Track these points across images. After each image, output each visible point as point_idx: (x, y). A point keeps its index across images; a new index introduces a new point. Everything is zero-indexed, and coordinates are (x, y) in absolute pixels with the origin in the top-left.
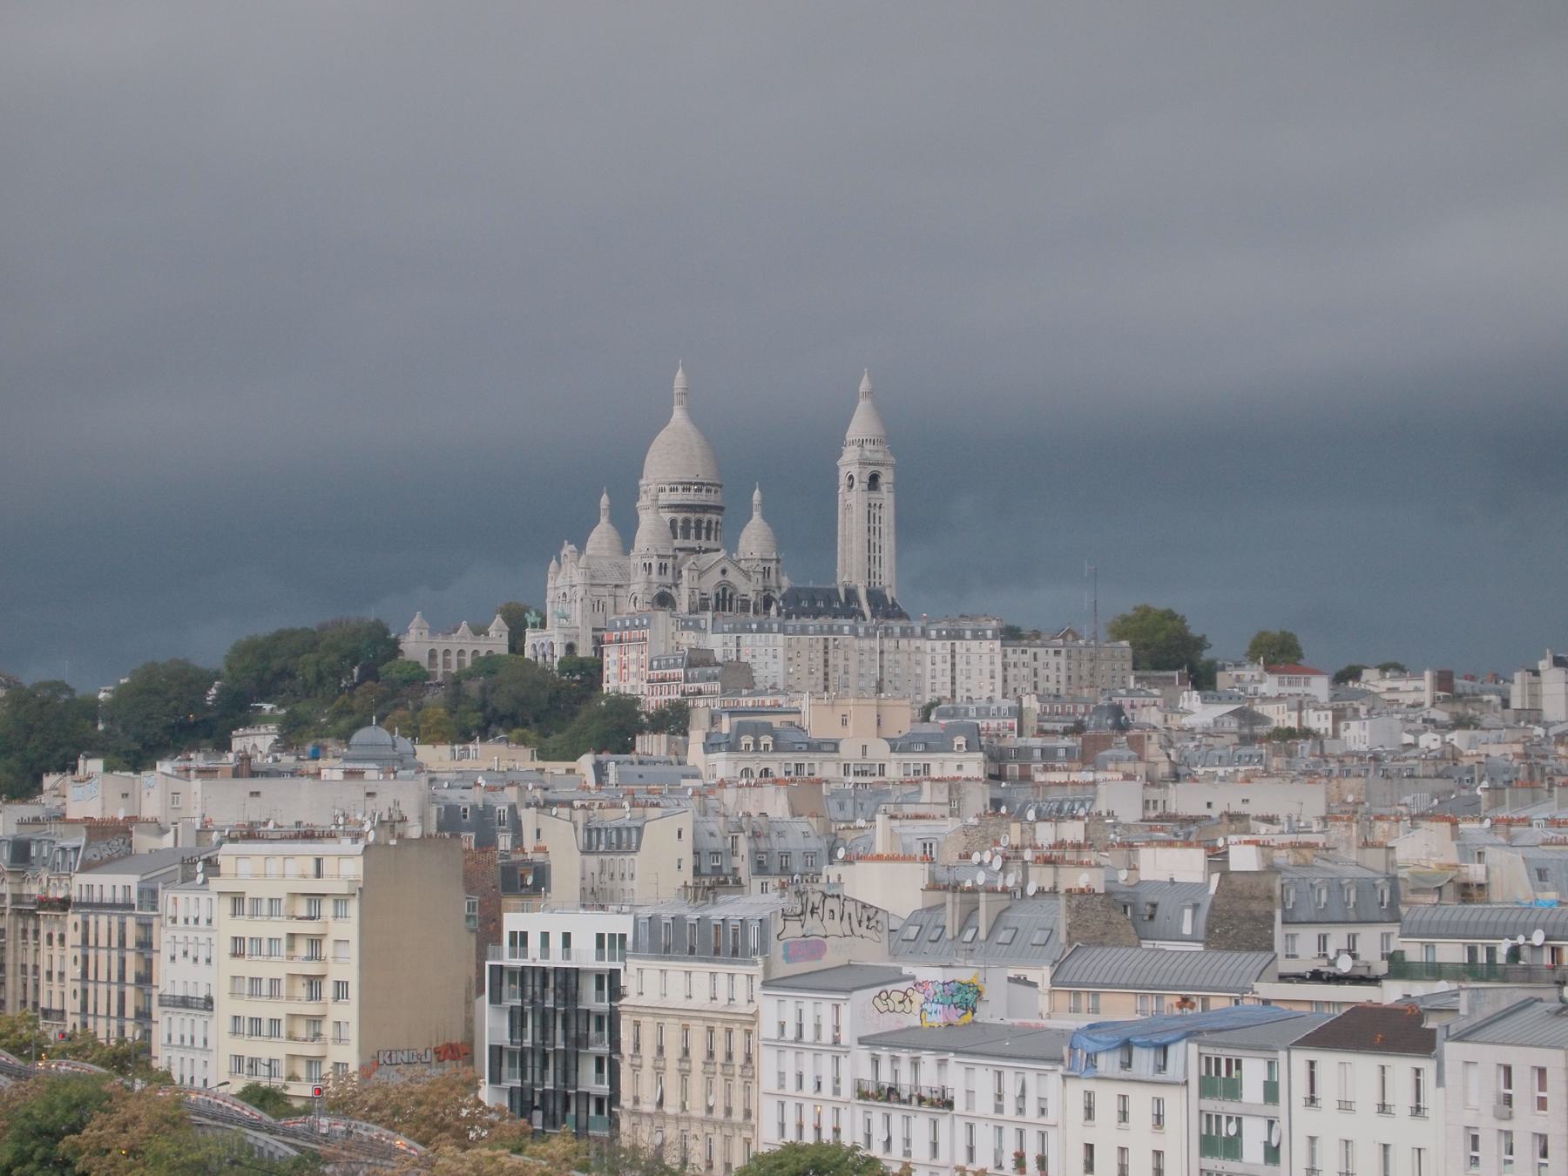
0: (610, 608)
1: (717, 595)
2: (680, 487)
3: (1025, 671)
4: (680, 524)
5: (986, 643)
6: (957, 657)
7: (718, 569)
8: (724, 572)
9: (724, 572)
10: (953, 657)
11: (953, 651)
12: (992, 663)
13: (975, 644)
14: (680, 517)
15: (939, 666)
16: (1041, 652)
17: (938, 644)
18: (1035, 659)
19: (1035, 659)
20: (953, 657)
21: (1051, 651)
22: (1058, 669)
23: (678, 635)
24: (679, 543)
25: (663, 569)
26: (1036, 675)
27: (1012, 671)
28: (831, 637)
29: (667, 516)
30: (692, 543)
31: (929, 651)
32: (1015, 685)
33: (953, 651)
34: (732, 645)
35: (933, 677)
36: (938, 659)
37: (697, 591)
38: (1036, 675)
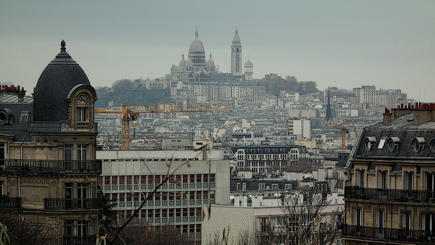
0: (181, 78)
1: (201, 75)
2: (195, 53)
3: (245, 92)
4: (195, 60)
5: (237, 87)
6: (232, 89)
7: (201, 69)
8: (202, 70)
9: (202, 70)
10: (231, 89)
11: (231, 88)
12: (238, 90)
13: (235, 87)
14: (195, 59)
15: (229, 91)
16: (248, 88)
17: (229, 87)
18: (247, 90)
19: (247, 90)
20: (231, 89)
21: (250, 88)
22: (251, 91)
23: (183, 85)
24: (194, 64)
25: (190, 70)
26: (247, 93)
27: (242, 92)
28: (210, 86)
29: (193, 59)
30: (198, 64)
31: (227, 88)
32: (243, 94)
33: (231, 88)
34: (192, 87)
35: (228, 93)
36: (229, 90)
37: (196, 74)
38: (247, 93)
